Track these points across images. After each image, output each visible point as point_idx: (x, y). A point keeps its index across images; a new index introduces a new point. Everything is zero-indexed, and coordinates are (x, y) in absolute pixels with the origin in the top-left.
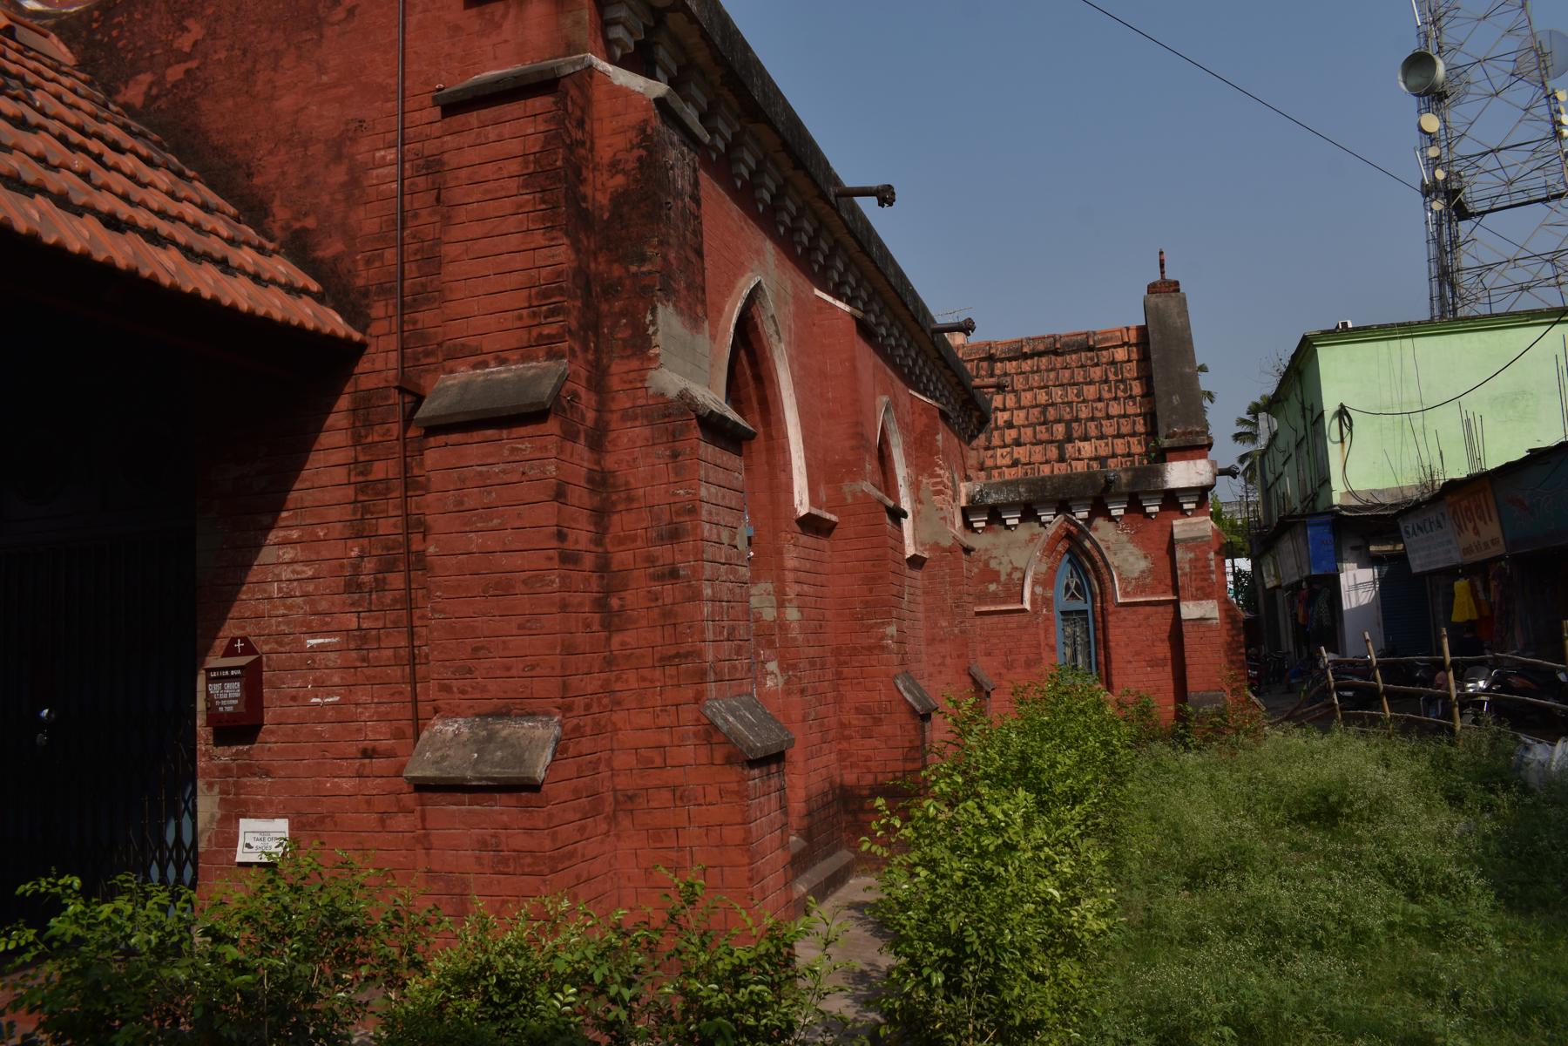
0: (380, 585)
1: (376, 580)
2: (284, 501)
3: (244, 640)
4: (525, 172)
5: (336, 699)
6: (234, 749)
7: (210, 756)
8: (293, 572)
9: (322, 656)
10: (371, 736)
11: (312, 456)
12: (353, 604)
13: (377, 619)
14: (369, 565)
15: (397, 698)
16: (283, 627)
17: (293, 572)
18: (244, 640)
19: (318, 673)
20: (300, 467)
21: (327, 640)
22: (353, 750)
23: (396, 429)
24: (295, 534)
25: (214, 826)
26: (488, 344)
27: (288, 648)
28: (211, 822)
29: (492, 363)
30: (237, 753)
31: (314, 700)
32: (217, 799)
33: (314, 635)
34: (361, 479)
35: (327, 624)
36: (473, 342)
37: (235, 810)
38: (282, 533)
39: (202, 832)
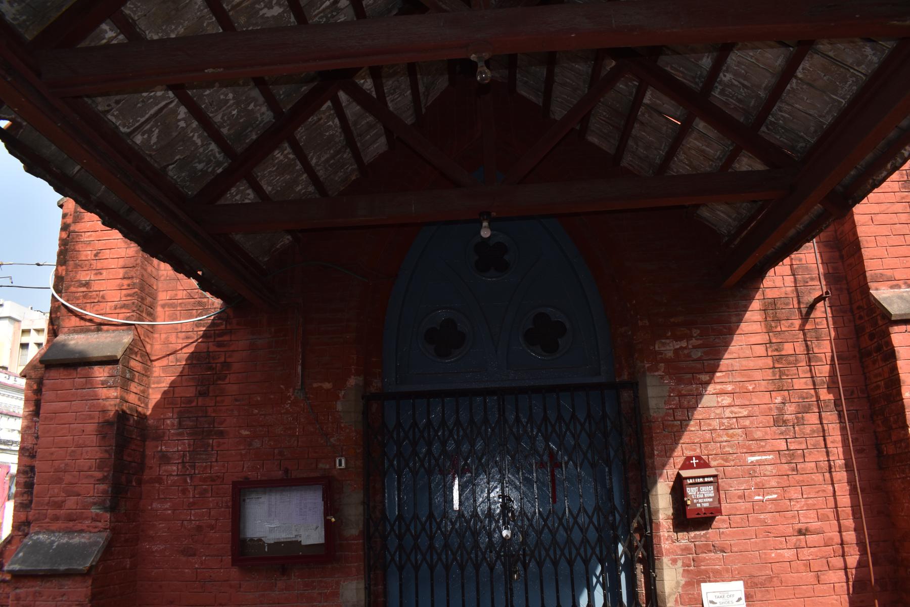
0: (800, 422)
1: (797, 418)
2: (718, 366)
3: (698, 458)
4: (902, 180)
5: (775, 496)
6: (692, 534)
8: (732, 412)
9: (762, 467)
10: (803, 520)
11: (736, 337)
12: (782, 433)
13: (801, 443)
14: (790, 409)
15: (821, 494)
16: (727, 449)
17: (732, 412)
18: (698, 458)
19: (758, 479)
20: (727, 345)
21: (764, 457)
22: (790, 530)
23: (797, 323)
24: (729, 388)
25: (680, 590)
26: (898, 274)
27: (732, 463)
28: (677, 587)
29: (903, 286)
30: (695, 537)
31: (757, 498)
32: (681, 570)
33: (753, 453)
34: (776, 353)
35: (762, 447)
36: (888, 273)
38: (719, 387)
39: (670, 595)
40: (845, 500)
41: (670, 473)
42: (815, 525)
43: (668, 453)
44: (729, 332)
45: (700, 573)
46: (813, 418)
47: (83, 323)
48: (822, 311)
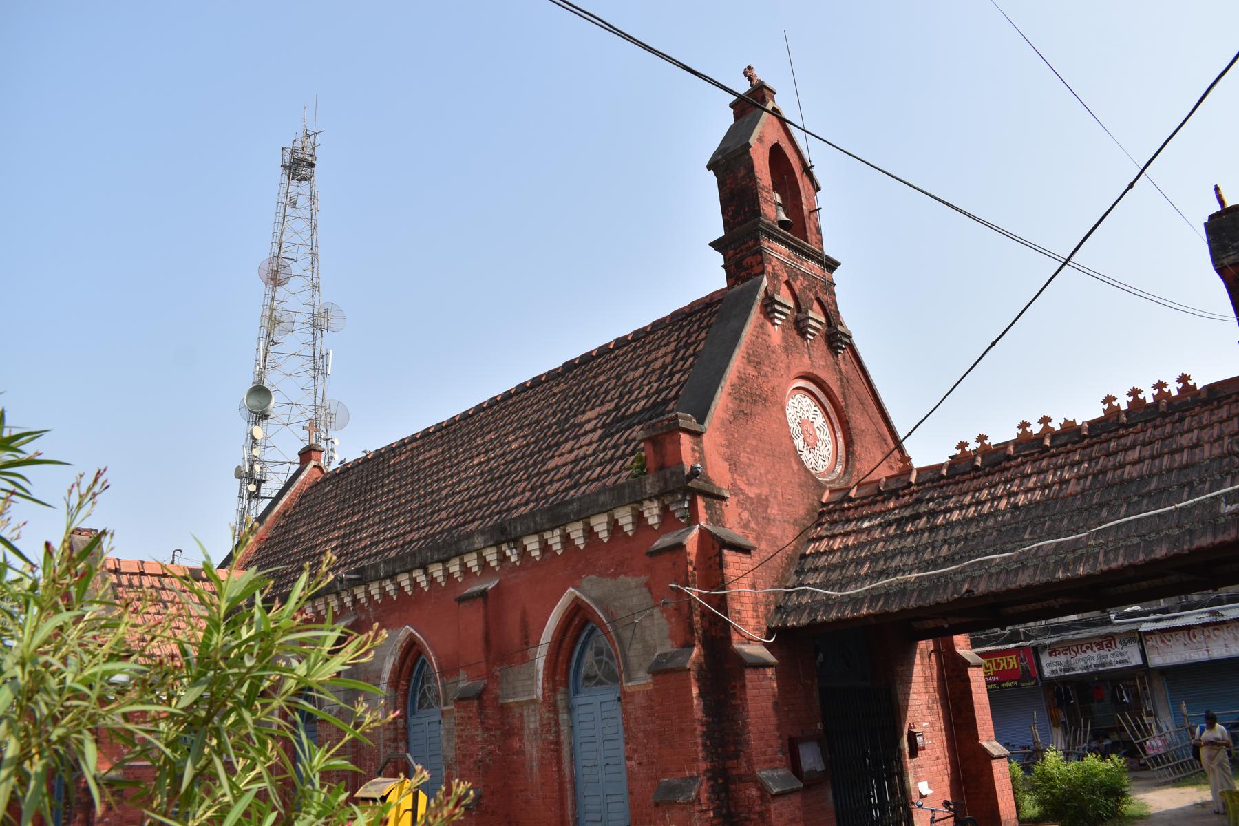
2: (911, 680)
7: (910, 763)
14: (930, 702)
24: (915, 690)
33: (924, 722)
37: (918, 779)
40: (945, 744)
41: (906, 731)
42: (940, 755)
43: (905, 723)
44: (912, 664)
45: (917, 777)
46: (935, 705)
47: (740, 638)
48: (933, 655)
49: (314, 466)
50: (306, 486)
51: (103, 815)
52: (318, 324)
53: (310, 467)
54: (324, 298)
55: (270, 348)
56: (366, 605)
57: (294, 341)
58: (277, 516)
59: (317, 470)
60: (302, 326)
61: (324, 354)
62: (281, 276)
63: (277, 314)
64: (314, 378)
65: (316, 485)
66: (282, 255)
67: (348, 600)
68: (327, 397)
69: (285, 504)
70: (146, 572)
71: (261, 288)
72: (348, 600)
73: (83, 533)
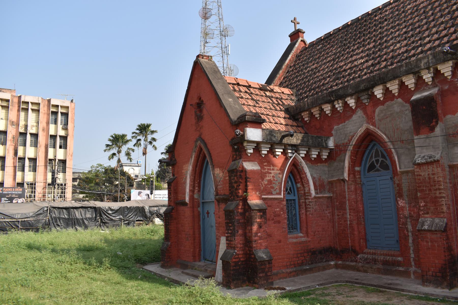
49: (302, 41)
50: (299, 51)
51: (257, 231)
52: (224, 34)
53: (299, 40)
54: (225, 23)
55: (206, 45)
56: (449, 77)
57: (214, 42)
58: (287, 66)
59: (302, 43)
60: (216, 36)
61: (227, 46)
62: (208, 15)
63: (207, 31)
64: (222, 57)
65: (305, 49)
66: (208, 7)
67: (427, 77)
68: (229, 63)
69: (290, 60)
70: (240, 84)
71: (200, 20)
72: (427, 77)
73: (205, 58)
